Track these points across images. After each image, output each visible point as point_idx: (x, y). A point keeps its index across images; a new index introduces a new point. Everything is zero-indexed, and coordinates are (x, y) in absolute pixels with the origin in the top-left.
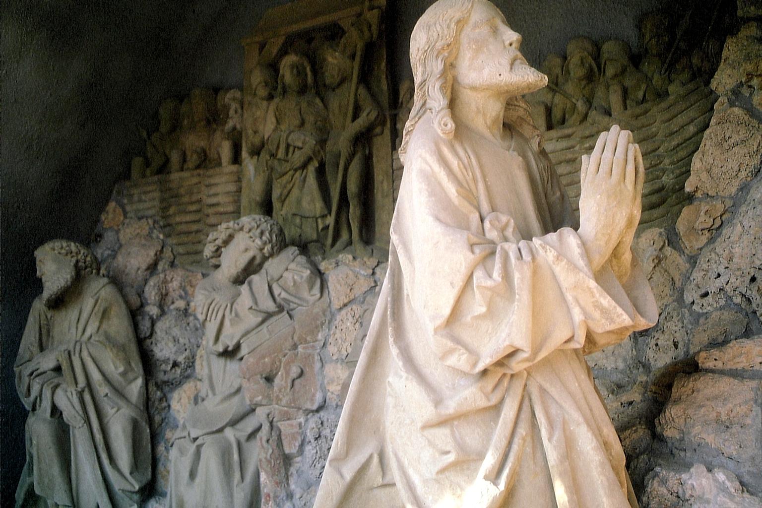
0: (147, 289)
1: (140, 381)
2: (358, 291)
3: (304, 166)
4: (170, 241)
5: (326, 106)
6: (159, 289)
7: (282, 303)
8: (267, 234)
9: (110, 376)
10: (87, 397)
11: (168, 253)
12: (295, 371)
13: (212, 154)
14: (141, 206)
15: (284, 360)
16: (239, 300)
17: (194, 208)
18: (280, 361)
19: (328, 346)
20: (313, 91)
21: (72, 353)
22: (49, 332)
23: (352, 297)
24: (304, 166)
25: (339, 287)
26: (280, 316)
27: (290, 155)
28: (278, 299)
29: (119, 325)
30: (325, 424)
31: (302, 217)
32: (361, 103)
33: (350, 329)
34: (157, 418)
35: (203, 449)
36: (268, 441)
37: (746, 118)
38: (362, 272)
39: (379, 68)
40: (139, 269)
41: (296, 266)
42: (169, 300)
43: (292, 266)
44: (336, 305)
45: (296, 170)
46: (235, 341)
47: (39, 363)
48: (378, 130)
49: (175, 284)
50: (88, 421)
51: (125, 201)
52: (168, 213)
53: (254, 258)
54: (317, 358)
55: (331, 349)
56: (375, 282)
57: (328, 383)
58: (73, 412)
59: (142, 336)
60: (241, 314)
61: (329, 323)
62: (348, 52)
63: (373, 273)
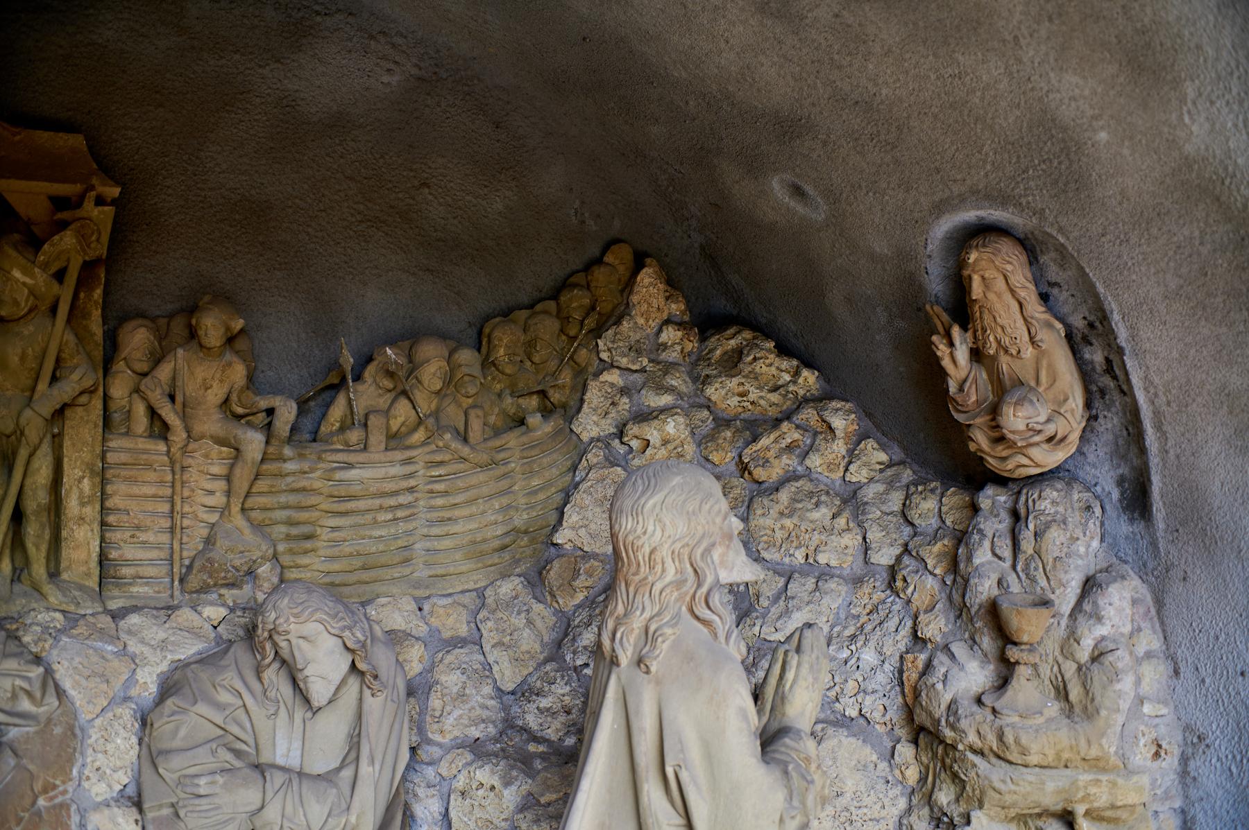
2: (117, 684)
19: (86, 784)
23: (111, 695)
25: (84, 682)
33: (122, 747)
38: (110, 648)
41: (19, 664)
55: (99, 790)
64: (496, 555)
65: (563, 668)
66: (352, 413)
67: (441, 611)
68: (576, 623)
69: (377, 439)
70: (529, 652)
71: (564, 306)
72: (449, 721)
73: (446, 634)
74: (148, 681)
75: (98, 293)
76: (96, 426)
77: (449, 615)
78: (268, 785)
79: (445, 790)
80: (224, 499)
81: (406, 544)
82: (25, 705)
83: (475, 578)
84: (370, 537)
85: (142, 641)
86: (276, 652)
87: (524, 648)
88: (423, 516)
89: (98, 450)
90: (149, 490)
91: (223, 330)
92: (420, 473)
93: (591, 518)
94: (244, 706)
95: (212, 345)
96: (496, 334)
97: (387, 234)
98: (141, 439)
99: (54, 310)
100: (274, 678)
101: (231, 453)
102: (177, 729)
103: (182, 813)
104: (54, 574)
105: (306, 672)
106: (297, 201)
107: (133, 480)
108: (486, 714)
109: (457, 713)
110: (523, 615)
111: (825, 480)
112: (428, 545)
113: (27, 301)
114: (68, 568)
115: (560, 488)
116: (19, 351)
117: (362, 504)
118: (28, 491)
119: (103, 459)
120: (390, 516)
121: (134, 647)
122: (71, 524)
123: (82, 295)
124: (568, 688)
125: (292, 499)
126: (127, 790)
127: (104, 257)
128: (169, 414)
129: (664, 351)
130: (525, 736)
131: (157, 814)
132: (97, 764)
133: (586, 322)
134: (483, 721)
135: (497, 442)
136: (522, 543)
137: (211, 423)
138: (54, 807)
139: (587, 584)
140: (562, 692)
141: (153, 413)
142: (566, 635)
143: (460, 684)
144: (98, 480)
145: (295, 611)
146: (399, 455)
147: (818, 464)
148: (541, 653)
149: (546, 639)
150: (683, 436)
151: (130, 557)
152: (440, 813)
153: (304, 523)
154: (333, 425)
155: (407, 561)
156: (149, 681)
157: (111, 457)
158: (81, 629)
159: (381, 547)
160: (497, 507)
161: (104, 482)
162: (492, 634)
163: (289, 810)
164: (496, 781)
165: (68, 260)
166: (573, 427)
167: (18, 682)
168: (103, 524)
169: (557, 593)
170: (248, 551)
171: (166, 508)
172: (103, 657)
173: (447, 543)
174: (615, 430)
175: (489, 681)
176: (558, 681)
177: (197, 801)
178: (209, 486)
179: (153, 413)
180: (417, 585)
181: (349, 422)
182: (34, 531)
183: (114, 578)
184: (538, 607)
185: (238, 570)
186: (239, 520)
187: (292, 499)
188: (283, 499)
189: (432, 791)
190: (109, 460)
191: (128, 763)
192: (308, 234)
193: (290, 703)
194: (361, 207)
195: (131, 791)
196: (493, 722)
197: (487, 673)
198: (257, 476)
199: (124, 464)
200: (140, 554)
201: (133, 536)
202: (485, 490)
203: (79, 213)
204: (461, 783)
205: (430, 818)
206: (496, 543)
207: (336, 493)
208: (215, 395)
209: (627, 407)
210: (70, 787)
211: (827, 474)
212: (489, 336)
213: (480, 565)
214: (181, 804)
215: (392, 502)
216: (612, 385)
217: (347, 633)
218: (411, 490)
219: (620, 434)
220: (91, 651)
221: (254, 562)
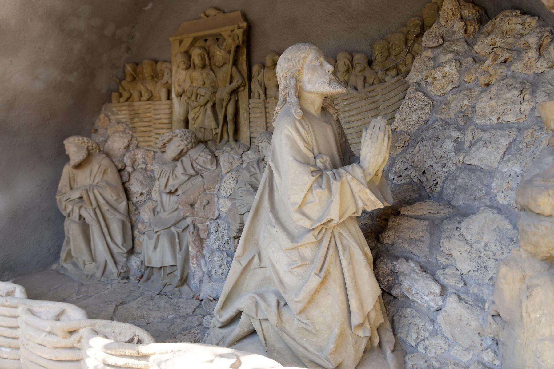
0: (125, 158)
1: (124, 203)
3: (205, 104)
4: (135, 135)
5: (216, 76)
6: (132, 159)
7: (198, 171)
8: (189, 138)
9: (109, 202)
10: (98, 211)
11: (135, 142)
12: (205, 202)
13: (155, 94)
15: (199, 197)
16: (177, 169)
18: (198, 197)
19: (221, 191)
20: (209, 67)
21: (89, 191)
22: (74, 180)
23: (232, 168)
24: (205, 104)
26: (197, 176)
27: (198, 98)
28: (196, 169)
29: (112, 176)
30: (220, 225)
31: (205, 129)
32: (233, 75)
34: (134, 219)
35: (160, 236)
36: (193, 233)
37: (424, 97)
38: (236, 157)
40: (120, 148)
42: (137, 164)
43: (202, 154)
44: (224, 172)
45: (201, 106)
46: (175, 188)
47: (70, 195)
48: (242, 89)
49: (140, 156)
50: (99, 222)
51: (110, 114)
52: (134, 122)
53: (183, 149)
54: (216, 196)
55: (223, 192)
56: (242, 161)
57: (221, 208)
58: (91, 218)
59: (125, 181)
60: (178, 175)
61: (221, 180)
62: (227, 50)
63: (241, 157)
82: (209, 167)
85: (248, 157)
89: (248, 104)
90: (258, 115)
91: (271, 60)
92: (340, 104)
97: (336, 18)
104: (236, 140)
107: (255, 113)
111: (524, 76)
127: (241, 44)
138: (210, 194)
144: (248, 113)
147: (519, 68)
150: (454, 72)
157: (251, 106)
158: (233, 152)
160: (370, 116)
167: (204, 159)
168: (250, 127)
172: (233, 159)
191: (232, 188)
211: (524, 72)
220: (230, 157)
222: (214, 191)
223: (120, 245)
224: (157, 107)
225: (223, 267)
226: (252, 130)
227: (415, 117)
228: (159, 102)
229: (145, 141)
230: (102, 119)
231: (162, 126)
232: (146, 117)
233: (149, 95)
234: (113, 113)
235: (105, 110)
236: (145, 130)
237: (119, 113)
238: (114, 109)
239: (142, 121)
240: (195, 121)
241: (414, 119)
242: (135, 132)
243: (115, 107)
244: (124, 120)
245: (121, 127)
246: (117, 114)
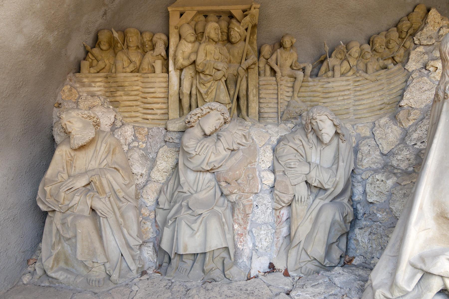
11: (119, 117)
14: (92, 89)
17: (135, 93)
39: (253, 38)
47: (74, 184)
62: (245, 27)
64: (378, 111)
65: (406, 146)
66: (329, 66)
67: (360, 128)
68: (410, 131)
69: (337, 73)
70: (392, 141)
71: (400, 28)
72: (365, 162)
73: (363, 135)
74: (274, 140)
75: (256, 36)
76: (256, 74)
77: (363, 129)
78: (311, 166)
79: (364, 184)
80: (292, 94)
81: (347, 107)
83: (371, 119)
84: (336, 105)
86: (312, 128)
87: (390, 140)
88: (353, 99)
89: (257, 81)
90: (271, 92)
93: (414, 95)
94: (303, 145)
95: (287, 47)
96: (376, 39)
98: (268, 77)
99: (245, 40)
100: (311, 136)
101: (293, 80)
102: (284, 150)
103: (286, 174)
105: (322, 132)
106: (308, 6)
107: (266, 89)
108: (377, 161)
109: (367, 160)
110: (390, 129)
112: (355, 108)
113: (238, 37)
114: (251, 114)
115: (401, 88)
116: (237, 51)
117: (333, 94)
118: (241, 91)
119: (259, 84)
120: (342, 98)
121: (270, 132)
122: (251, 102)
123: (251, 37)
124: (408, 152)
125: (311, 94)
126: (270, 168)
128: (276, 68)
129: (441, 37)
130: (392, 168)
131: (279, 174)
132: (262, 159)
133: (409, 31)
134: (377, 163)
135: (378, 73)
136: (387, 108)
137: (287, 71)
139: (414, 118)
140: (406, 154)
141: (272, 69)
142: (406, 136)
143: (368, 150)
144: (257, 90)
145: (318, 112)
146: (344, 78)
148: (397, 142)
149: (398, 138)
151: (266, 111)
152: (363, 191)
153: (315, 101)
154: (322, 72)
155: (348, 113)
156: (274, 140)
157: (261, 83)
159: (339, 108)
160: (378, 95)
161: (259, 90)
162: (378, 135)
163: (318, 174)
164: (383, 179)
165: (248, 25)
166: (405, 67)
168: (259, 102)
169: (402, 122)
170: (300, 107)
171: (276, 97)
173: (361, 107)
174: (422, 66)
175: (378, 150)
176: (404, 150)
177: (291, 169)
178: (287, 90)
179: (272, 69)
180: (351, 121)
181: (328, 70)
182: (243, 102)
183: (262, 118)
184: (395, 127)
185: (297, 113)
186: (296, 98)
187: (311, 94)
188: (309, 94)
189: (359, 184)
190: (260, 84)
191: (270, 160)
192: (312, 16)
193: (316, 145)
194: (328, 5)
195: (271, 168)
196: (380, 163)
197: (377, 148)
198: (301, 87)
199: (264, 85)
200: (269, 110)
201: (267, 105)
202: (374, 89)
203: (251, 12)
204: (370, 181)
205: (359, 193)
206: (379, 107)
207: (325, 91)
208: (288, 63)
209: (427, 58)
210: (256, 164)
212: (373, 41)
213: (373, 114)
214: (286, 170)
215: (343, 93)
216: (420, 52)
217: (334, 120)
218: (349, 90)
219: (425, 67)
221: (302, 110)
222: (255, 165)
223: (135, 236)
224: (149, 80)
225: (268, 240)
226: (262, 105)
227: (423, 96)
228: (153, 75)
229: (131, 117)
230: (66, 91)
231: (155, 100)
232: (132, 91)
233: (134, 67)
234: (83, 85)
235: (70, 80)
236: (132, 105)
237: (93, 85)
238: (85, 80)
239: (128, 95)
240: (208, 95)
241: (423, 98)
242: (117, 107)
243: (87, 77)
244: (99, 93)
245: (97, 101)
246: (90, 86)
